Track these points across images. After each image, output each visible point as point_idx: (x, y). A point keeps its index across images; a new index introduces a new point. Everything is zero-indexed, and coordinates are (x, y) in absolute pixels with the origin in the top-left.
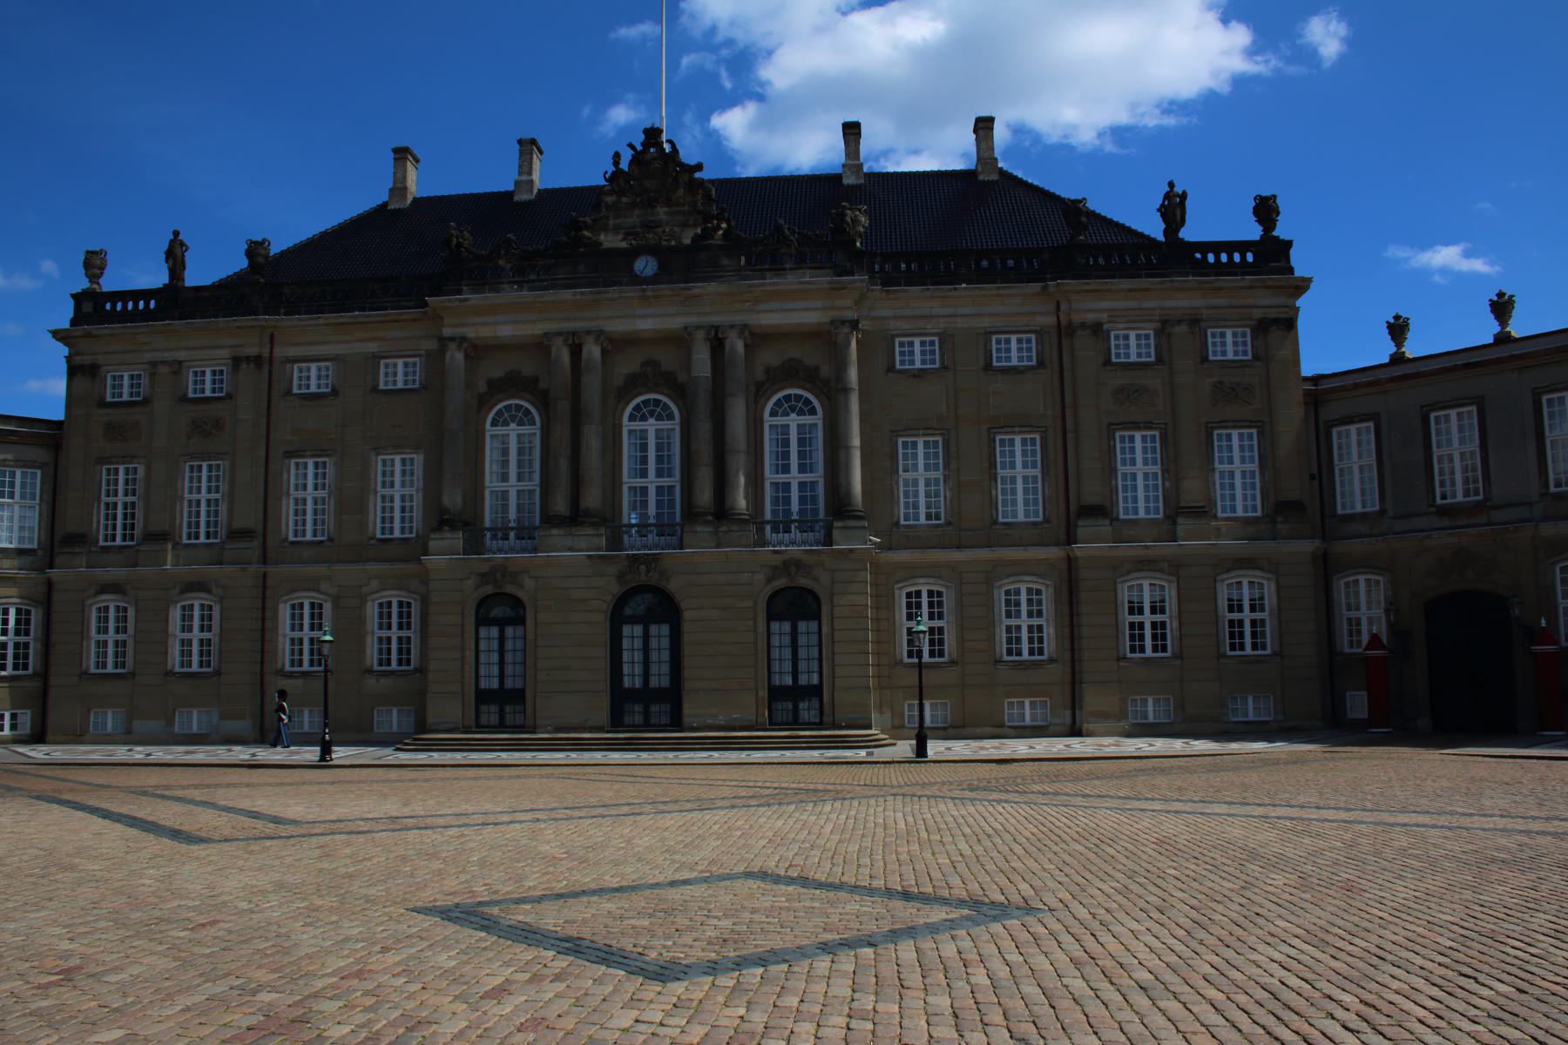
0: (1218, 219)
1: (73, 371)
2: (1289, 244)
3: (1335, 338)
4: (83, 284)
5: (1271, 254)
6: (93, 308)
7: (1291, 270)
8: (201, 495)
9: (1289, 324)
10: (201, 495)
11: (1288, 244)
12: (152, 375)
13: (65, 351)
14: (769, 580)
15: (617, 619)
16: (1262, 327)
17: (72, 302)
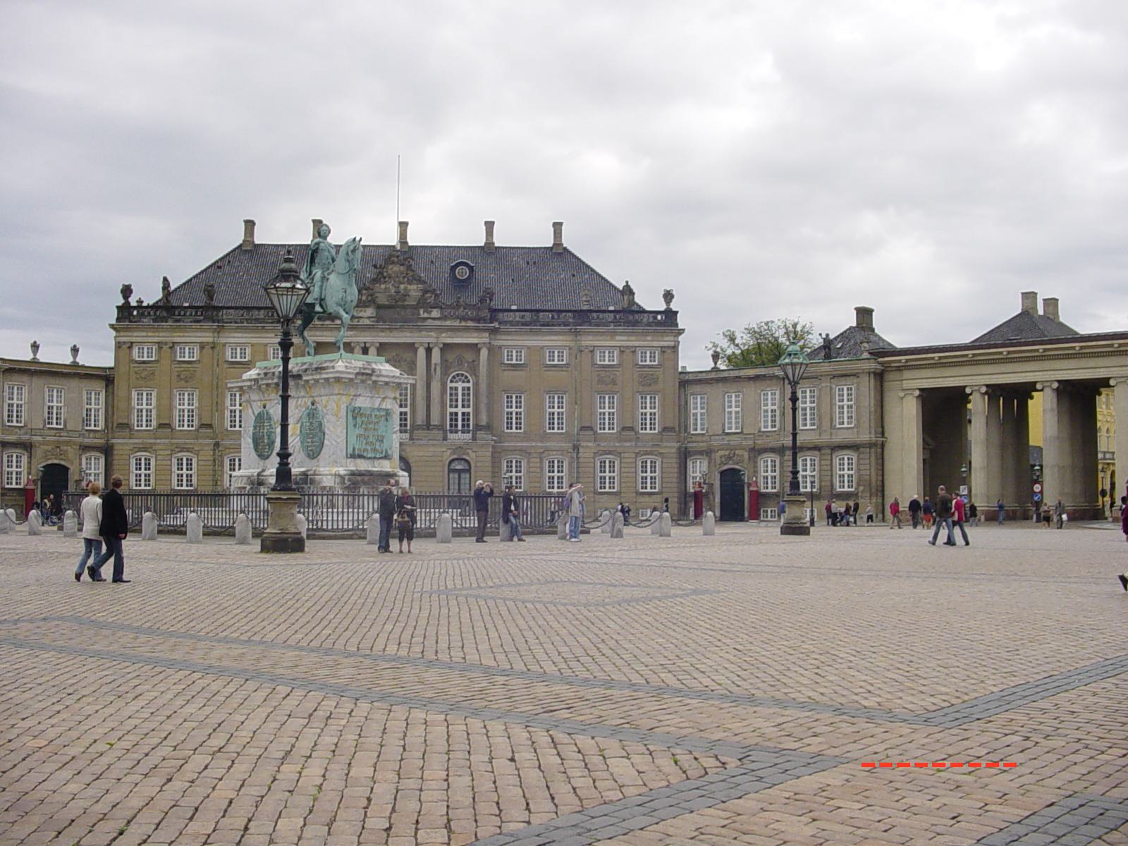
0: (650, 301)
1: (119, 346)
2: (676, 313)
3: (694, 357)
4: (121, 302)
5: (671, 315)
6: (128, 314)
7: (677, 325)
8: (186, 405)
9: (675, 349)
10: (186, 405)
11: (676, 313)
12: (160, 348)
13: (113, 333)
14: (451, 454)
16: (663, 350)
17: (116, 310)
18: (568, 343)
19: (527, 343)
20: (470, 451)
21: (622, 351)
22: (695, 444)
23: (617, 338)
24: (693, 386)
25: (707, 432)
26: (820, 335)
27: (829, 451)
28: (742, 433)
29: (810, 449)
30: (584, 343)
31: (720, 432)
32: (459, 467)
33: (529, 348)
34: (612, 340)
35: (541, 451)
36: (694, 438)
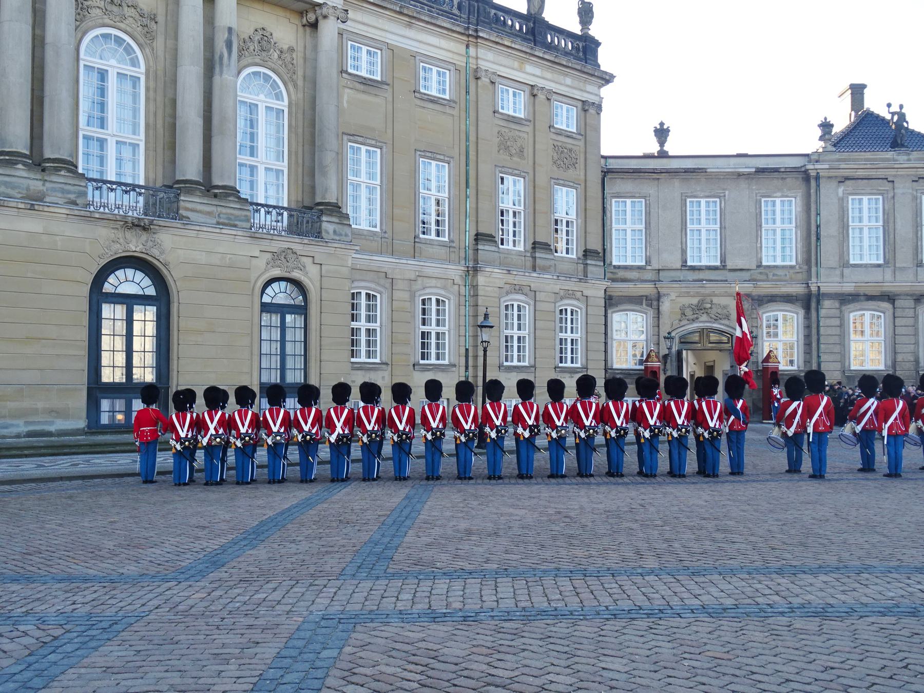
15: (98, 296)
18: (461, 62)
19: (392, 39)
20: (307, 261)
21: (533, 92)
22: (631, 285)
23: (529, 68)
24: (618, 181)
25: (648, 262)
26: (889, 105)
27: (910, 303)
28: (723, 267)
29: (870, 298)
30: (483, 65)
31: (678, 265)
32: (281, 299)
33: (391, 49)
34: (521, 70)
35: (413, 277)
36: (621, 274)
